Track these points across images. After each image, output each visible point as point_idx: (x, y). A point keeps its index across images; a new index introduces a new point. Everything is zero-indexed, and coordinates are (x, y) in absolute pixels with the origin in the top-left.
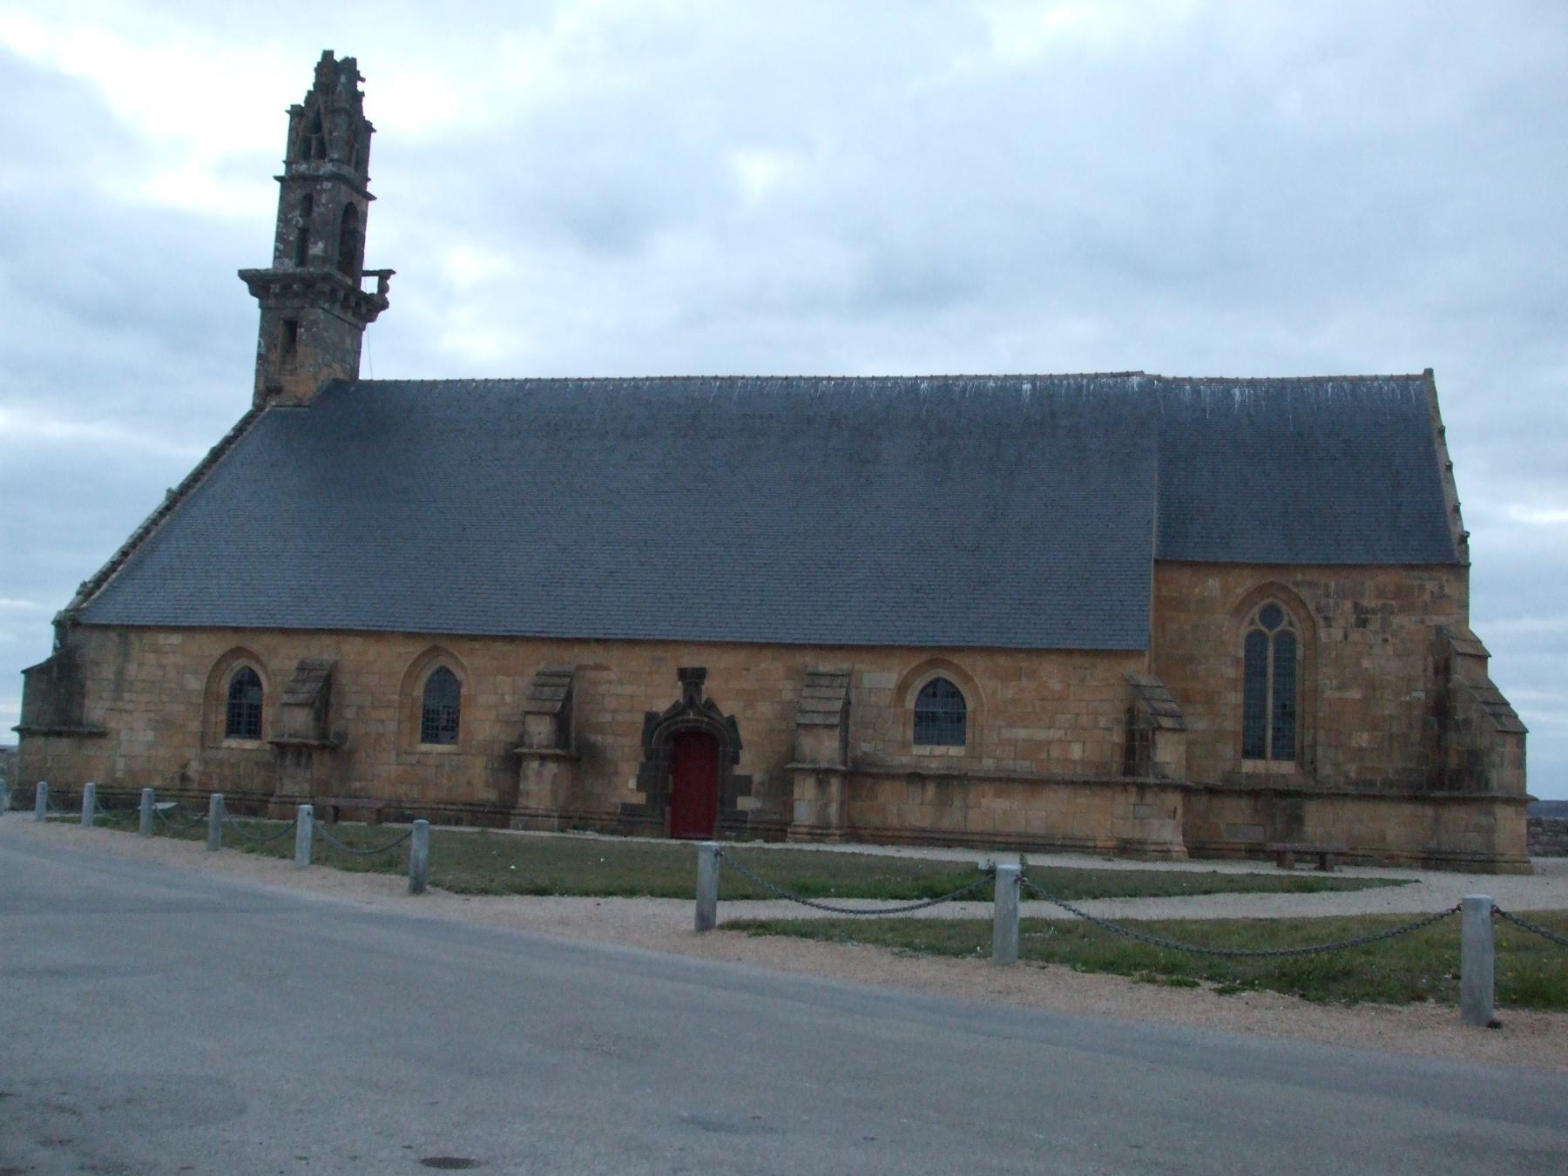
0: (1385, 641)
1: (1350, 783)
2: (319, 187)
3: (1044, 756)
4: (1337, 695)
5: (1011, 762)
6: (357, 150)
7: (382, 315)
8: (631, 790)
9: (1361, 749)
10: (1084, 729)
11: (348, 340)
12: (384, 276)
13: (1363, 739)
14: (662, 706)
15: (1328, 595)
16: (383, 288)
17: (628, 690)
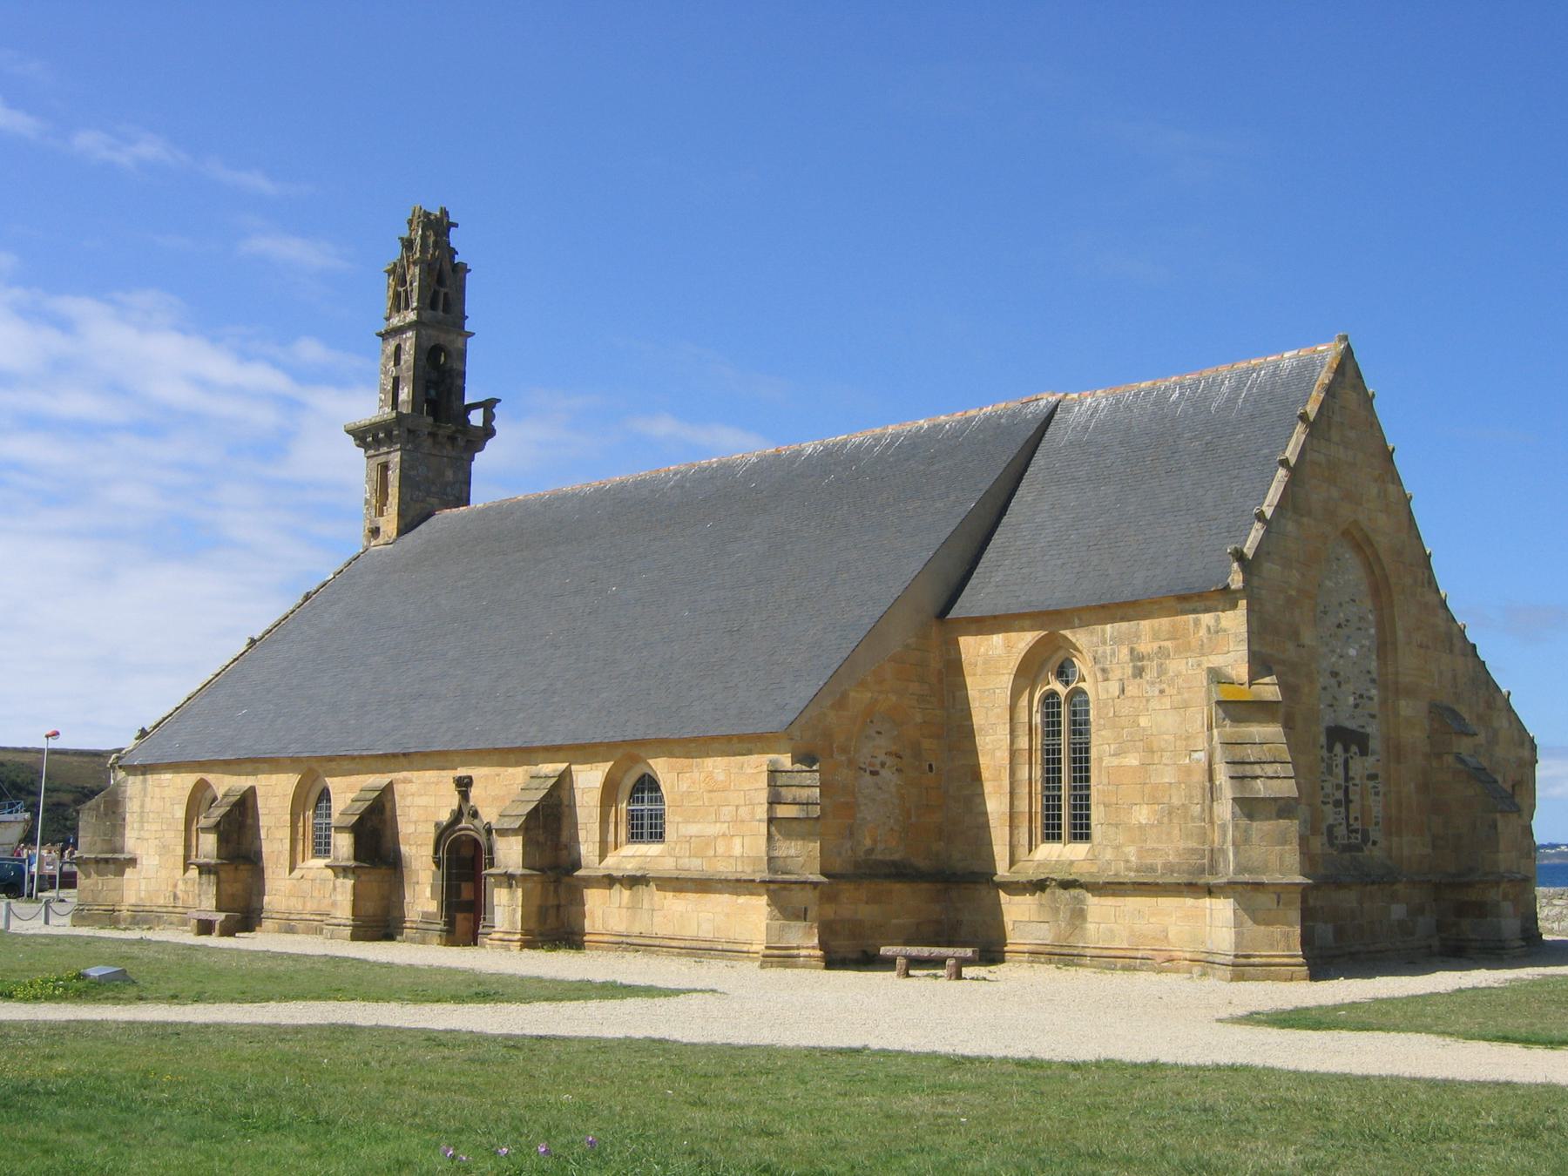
0: (1162, 692)
1: (1129, 869)
2: (404, 336)
4: (1115, 762)
5: (687, 860)
6: (446, 294)
7: (490, 443)
9: (1141, 827)
10: (743, 821)
11: (449, 474)
12: (488, 406)
14: (445, 817)
16: (489, 418)
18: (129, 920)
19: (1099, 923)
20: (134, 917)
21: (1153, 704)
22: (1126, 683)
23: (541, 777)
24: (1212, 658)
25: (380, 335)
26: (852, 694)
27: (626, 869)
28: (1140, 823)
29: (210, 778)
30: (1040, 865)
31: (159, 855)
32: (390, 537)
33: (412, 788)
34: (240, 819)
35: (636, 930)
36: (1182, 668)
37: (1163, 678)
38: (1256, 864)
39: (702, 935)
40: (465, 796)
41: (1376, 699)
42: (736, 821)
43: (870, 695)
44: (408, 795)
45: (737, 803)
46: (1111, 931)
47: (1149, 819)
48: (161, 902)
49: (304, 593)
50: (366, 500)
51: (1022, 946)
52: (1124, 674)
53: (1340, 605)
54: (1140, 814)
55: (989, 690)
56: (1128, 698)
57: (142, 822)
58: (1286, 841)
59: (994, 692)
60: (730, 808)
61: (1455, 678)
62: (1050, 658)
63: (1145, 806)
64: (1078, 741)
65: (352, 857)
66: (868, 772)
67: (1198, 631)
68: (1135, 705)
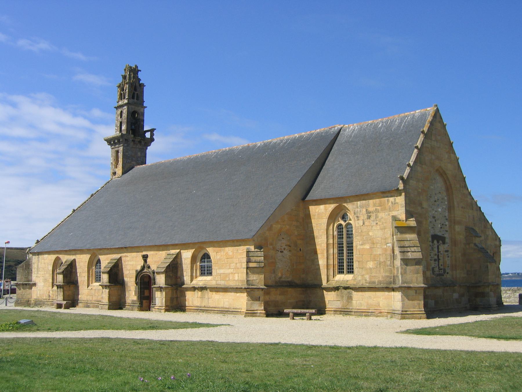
0: (377, 224)
2: (123, 108)
3: (228, 279)
4: (362, 247)
5: (220, 281)
6: (137, 94)
7: (153, 143)
8: (133, 296)
9: (370, 269)
10: (238, 268)
12: (152, 131)
13: (371, 265)
14: (139, 268)
15: (357, 207)
16: (152, 135)
17: (132, 263)
18: (34, 304)
19: (357, 301)
20: (35, 303)
21: (374, 228)
22: (365, 221)
23: (171, 255)
24: (393, 212)
25: (115, 108)
26: (274, 226)
27: (199, 285)
28: (370, 267)
29: (61, 256)
30: (337, 281)
31: (44, 282)
32: (119, 175)
33: (128, 259)
34: (70, 270)
35: (203, 305)
36: (383, 216)
37: (377, 219)
38: (408, 280)
39: (225, 306)
40: (145, 261)
41: (448, 226)
42: (236, 268)
43: (280, 226)
44: (126, 261)
45: (236, 262)
46: (361, 303)
47: (373, 266)
48: (45, 298)
49: (91, 194)
50: (111, 163)
51: (331, 309)
52: (364, 218)
53: (436, 194)
54: (370, 264)
55: (319, 224)
56: (365, 226)
57: (38, 271)
58: (418, 273)
59: (321, 225)
60: (234, 264)
61: (474, 218)
62: (339, 213)
63: (372, 262)
64: (349, 240)
65: (108, 282)
66: (280, 251)
67: (389, 203)
68: (368, 228)
